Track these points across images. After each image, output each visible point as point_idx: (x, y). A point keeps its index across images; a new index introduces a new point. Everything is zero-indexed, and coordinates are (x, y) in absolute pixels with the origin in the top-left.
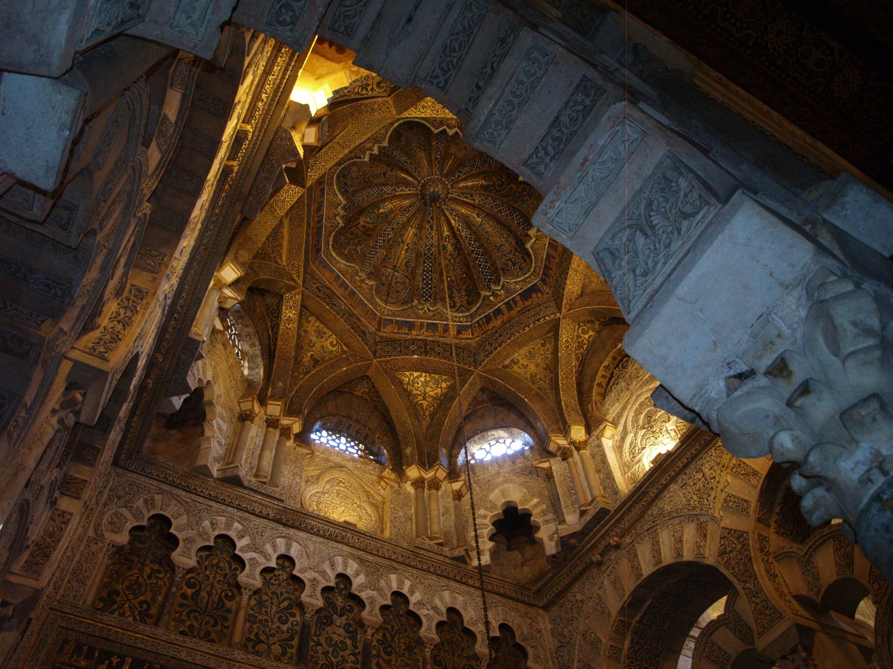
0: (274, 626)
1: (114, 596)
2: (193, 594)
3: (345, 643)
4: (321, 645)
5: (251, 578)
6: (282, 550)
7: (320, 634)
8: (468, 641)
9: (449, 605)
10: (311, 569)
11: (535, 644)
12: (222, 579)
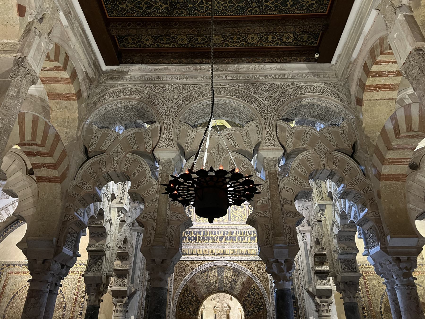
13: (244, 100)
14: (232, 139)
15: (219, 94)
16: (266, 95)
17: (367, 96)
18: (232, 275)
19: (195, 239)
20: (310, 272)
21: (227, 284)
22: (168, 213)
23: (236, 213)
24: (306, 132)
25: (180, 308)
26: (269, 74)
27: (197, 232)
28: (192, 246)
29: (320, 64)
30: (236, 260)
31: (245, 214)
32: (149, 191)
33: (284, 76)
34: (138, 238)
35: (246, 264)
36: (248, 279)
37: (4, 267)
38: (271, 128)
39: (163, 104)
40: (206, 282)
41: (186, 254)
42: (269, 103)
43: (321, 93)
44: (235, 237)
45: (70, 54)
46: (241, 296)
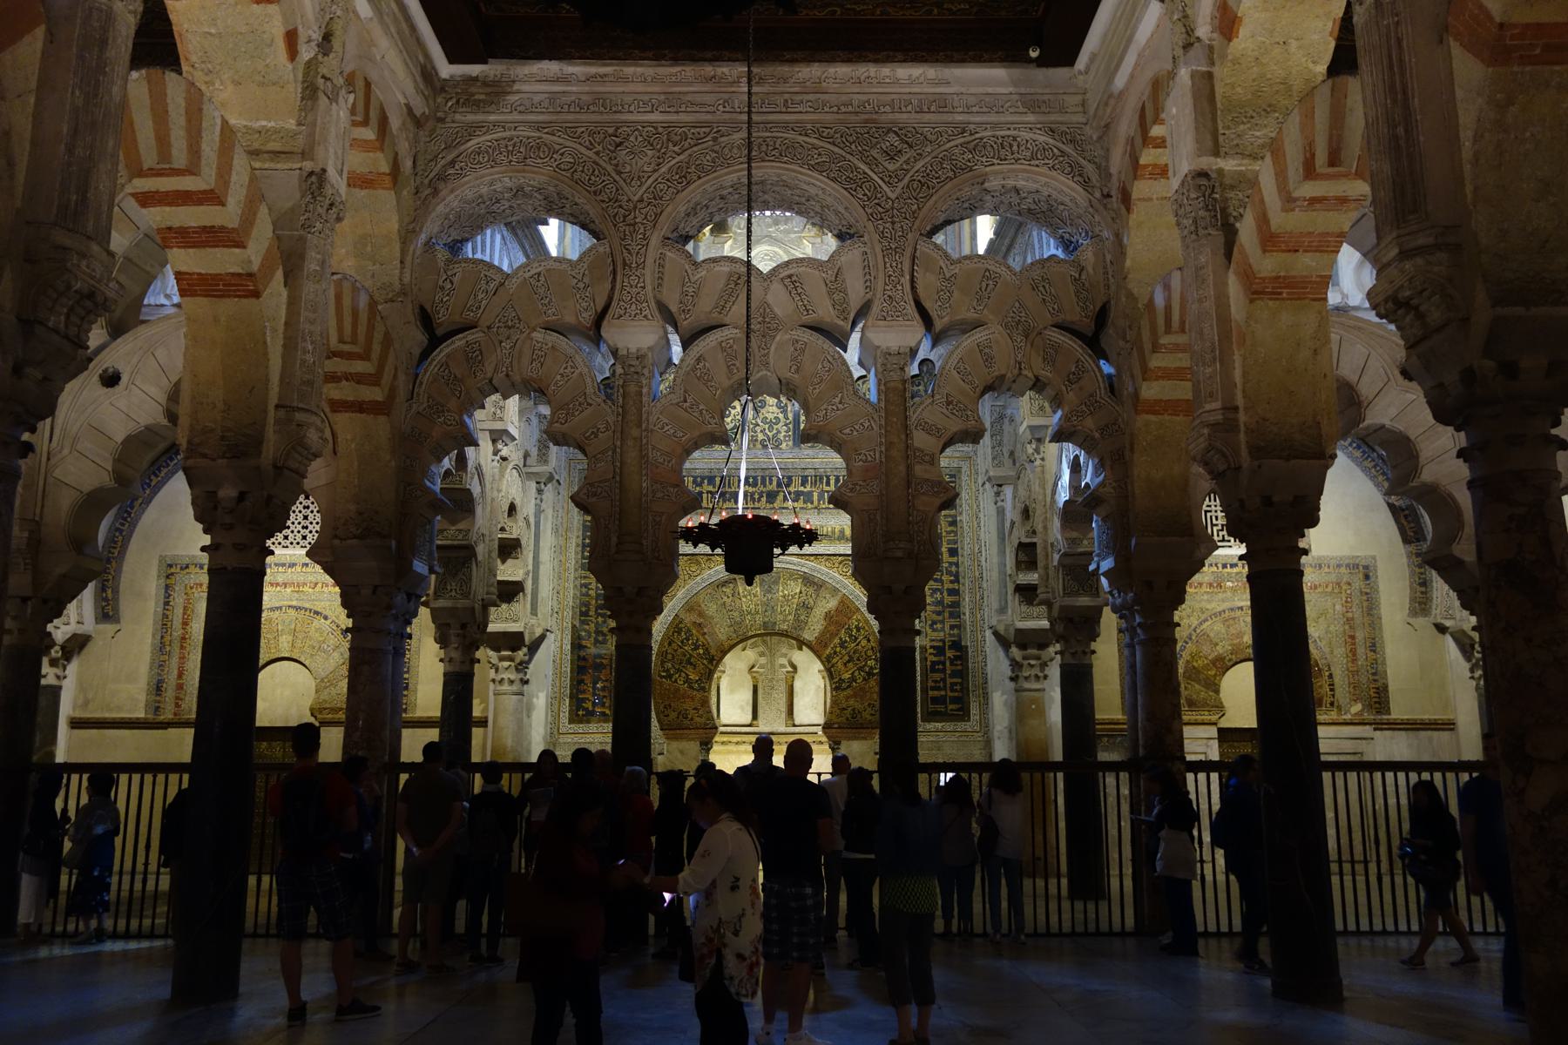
13: (834, 180)
14: (800, 290)
15: (767, 158)
16: (891, 167)
17: (1140, 189)
18: (801, 592)
20: (1006, 587)
21: (786, 616)
22: (644, 485)
24: (987, 274)
26: (905, 97)
27: (703, 478)
29: (1044, 70)
32: (595, 430)
33: (942, 104)
34: (539, 497)
36: (842, 602)
37: (173, 570)
38: (899, 266)
39: (617, 190)
42: (898, 191)
43: (1037, 162)
44: (811, 493)
45: (374, 76)
46: (823, 644)
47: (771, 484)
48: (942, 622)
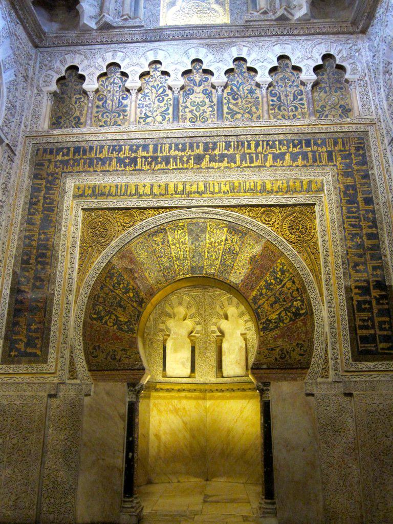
0: (156, 105)
1: (60, 120)
2: (103, 104)
3: (204, 101)
4: (188, 107)
5: (133, 82)
6: (152, 59)
7: (186, 101)
8: (297, 75)
9: (279, 55)
10: (172, 63)
11: (353, 61)
12: (118, 89)
18: (226, 240)
19: (134, 161)
23: (236, 105)
25: (95, 316)
27: (138, 147)
28: (125, 177)
30: (236, 206)
31: (260, 107)
35: (263, 213)
36: (265, 248)
40: (161, 257)
41: (110, 194)
47: (198, 147)
48: (364, 264)
